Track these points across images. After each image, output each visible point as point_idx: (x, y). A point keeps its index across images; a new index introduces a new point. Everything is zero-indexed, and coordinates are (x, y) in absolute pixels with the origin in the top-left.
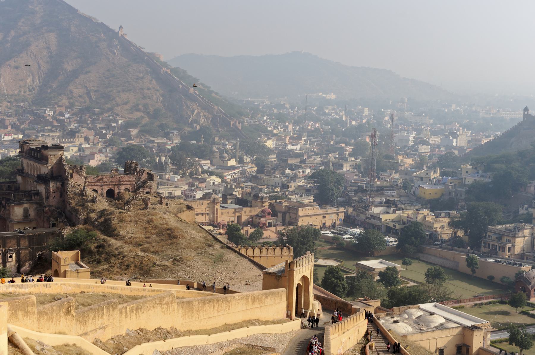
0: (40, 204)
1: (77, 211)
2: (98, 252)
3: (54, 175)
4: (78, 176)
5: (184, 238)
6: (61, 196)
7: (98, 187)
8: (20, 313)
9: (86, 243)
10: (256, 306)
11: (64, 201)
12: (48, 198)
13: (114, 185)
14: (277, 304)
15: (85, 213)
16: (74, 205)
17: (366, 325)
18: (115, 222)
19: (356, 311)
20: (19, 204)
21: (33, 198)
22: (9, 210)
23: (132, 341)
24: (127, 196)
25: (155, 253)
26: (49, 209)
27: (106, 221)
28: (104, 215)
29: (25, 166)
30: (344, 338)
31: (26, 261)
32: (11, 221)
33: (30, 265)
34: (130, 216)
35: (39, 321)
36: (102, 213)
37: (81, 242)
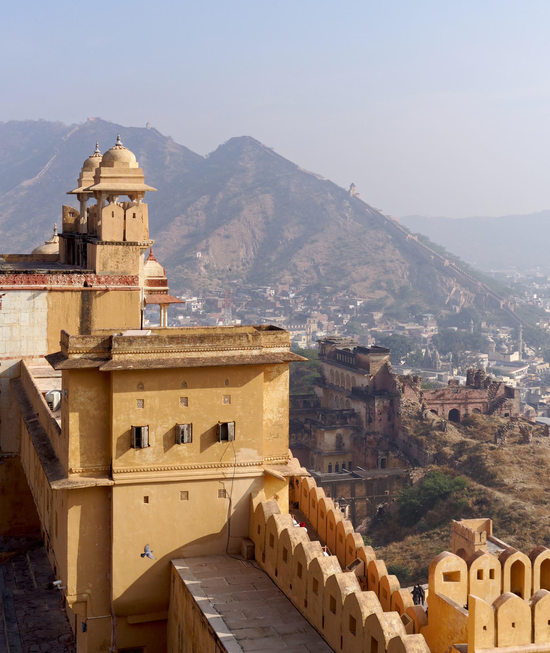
0: (357, 429)
1: (420, 444)
2: (480, 510)
3: (377, 389)
4: (411, 391)
6: (389, 419)
7: (438, 406)
11: (393, 426)
12: (370, 421)
13: (460, 404)
15: (433, 446)
16: (411, 433)
18: (490, 463)
20: (331, 428)
21: (348, 421)
22: (315, 437)
24: (481, 419)
26: (375, 438)
27: (470, 459)
28: (465, 451)
29: (327, 374)
31: (362, 517)
32: (319, 453)
33: (367, 523)
34: (507, 454)
36: (460, 447)
37: (448, 493)
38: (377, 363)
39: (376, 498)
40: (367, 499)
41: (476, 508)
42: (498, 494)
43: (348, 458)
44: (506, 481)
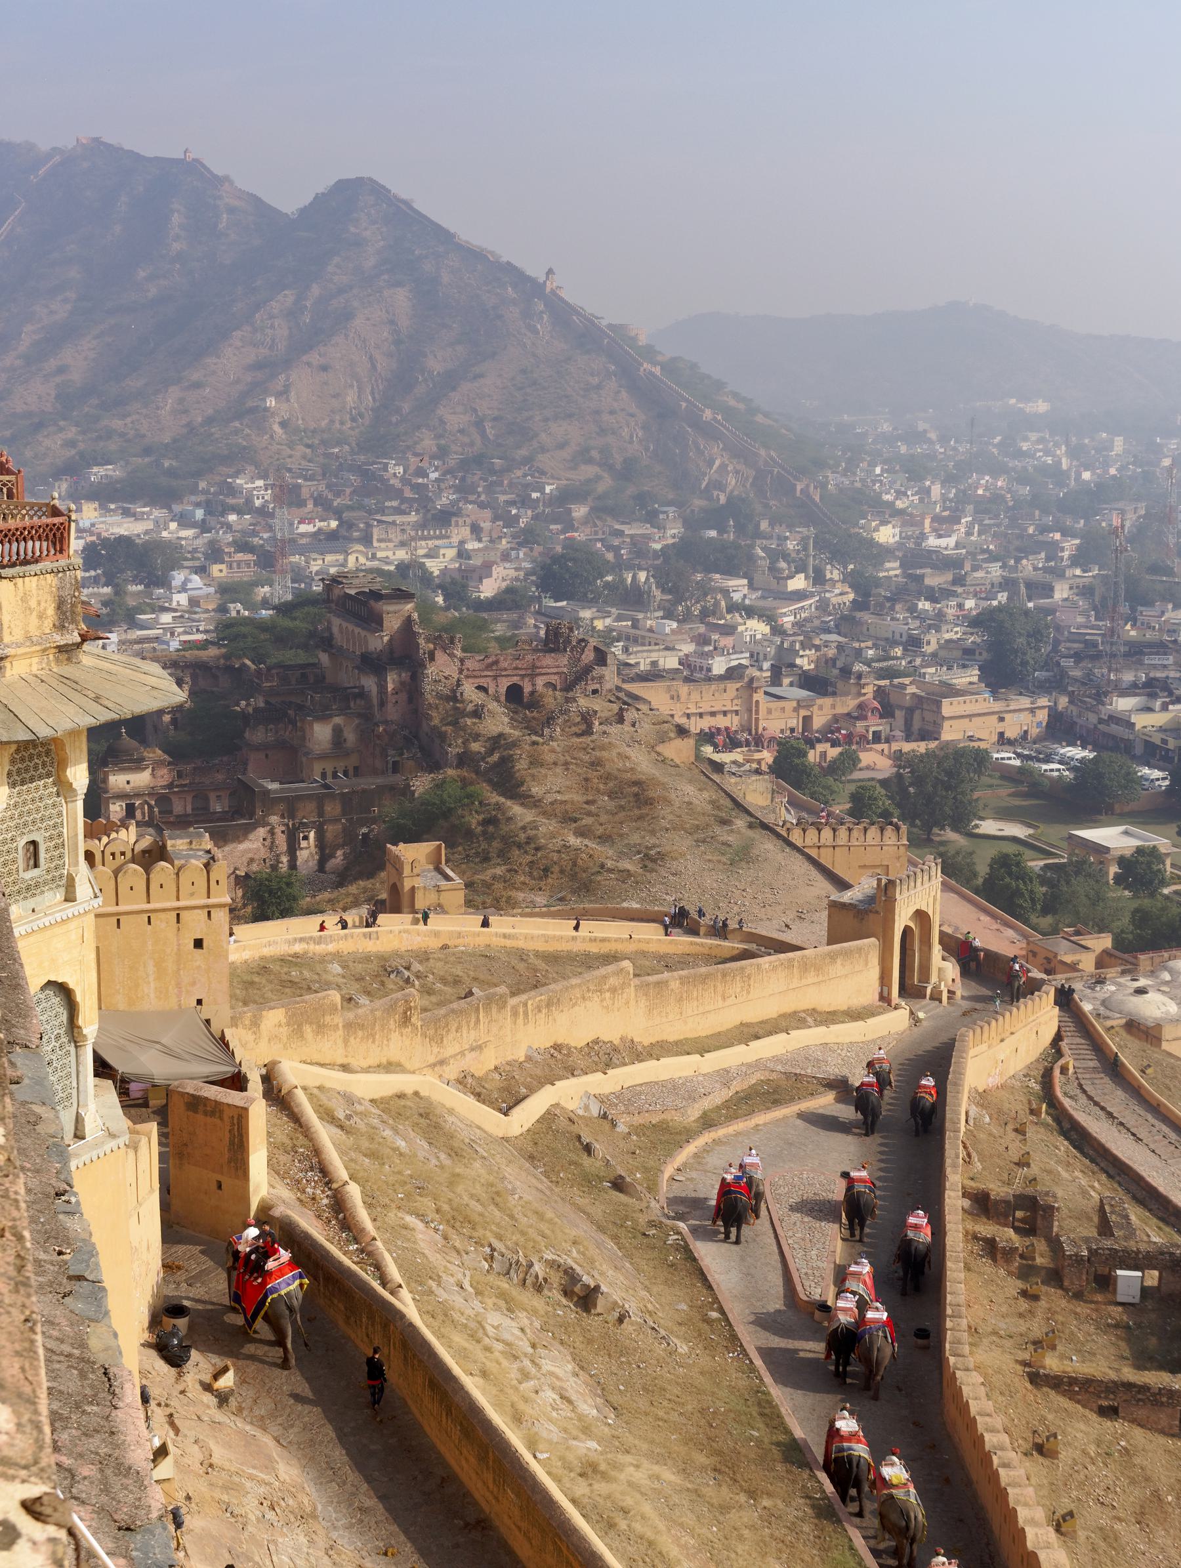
0: (366, 717)
1: (443, 737)
2: (484, 833)
5: (669, 802)
6: (410, 700)
7: (489, 680)
8: (308, 1030)
9: (460, 812)
10: (810, 981)
12: (382, 704)
13: (523, 676)
14: (856, 975)
15: (460, 741)
16: (436, 722)
17: (1056, 1020)
18: (521, 765)
19: (1034, 987)
20: (324, 718)
21: (352, 705)
22: (303, 730)
23: (539, 1072)
24: (551, 700)
25: (605, 839)
26: (384, 730)
28: (499, 748)
29: (335, 630)
30: (1003, 1051)
33: (344, 854)
34: (553, 751)
35: (346, 1042)
36: (497, 741)
37: (450, 810)
38: (394, 616)
42: (516, 809)
43: (353, 761)
44: (534, 790)
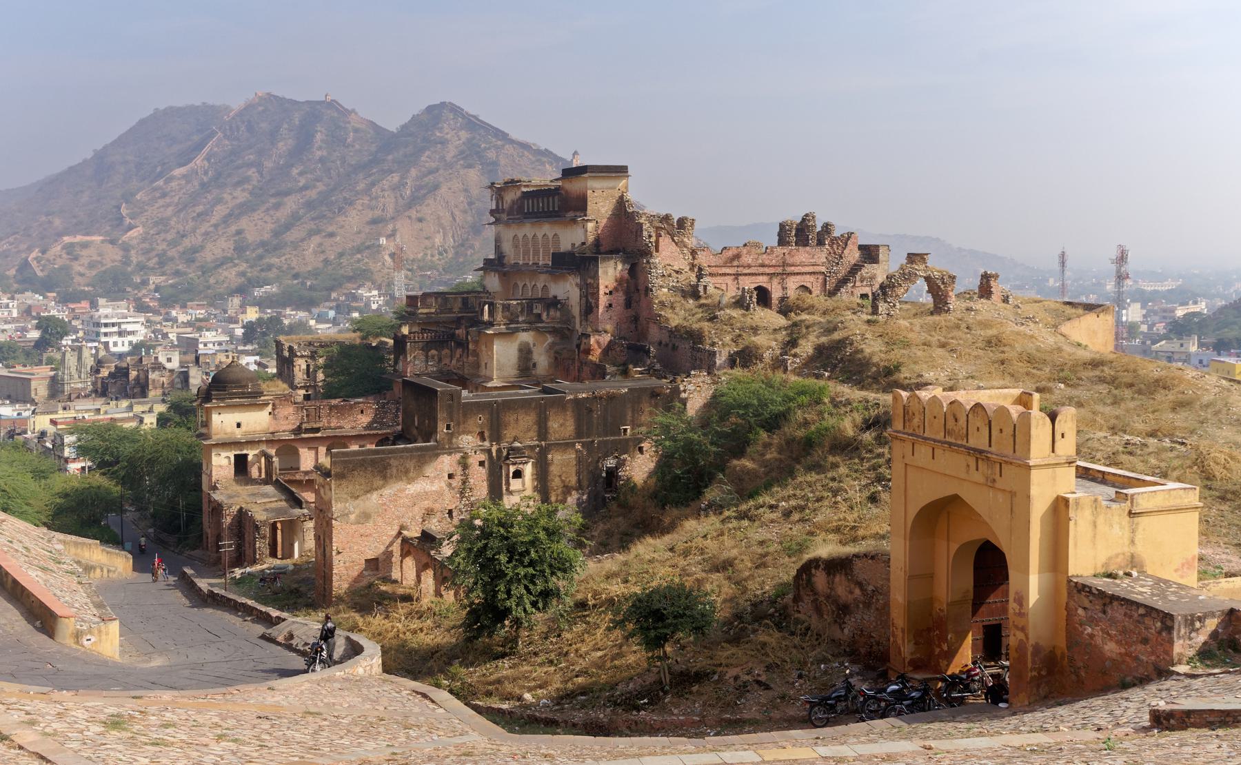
4: (673, 247)
6: (628, 304)
7: (729, 280)
11: (636, 319)
13: (771, 275)
15: (728, 339)
31: (567, 490)
39: (599, 442)
40: (578, 446)
41: (868, 437)
